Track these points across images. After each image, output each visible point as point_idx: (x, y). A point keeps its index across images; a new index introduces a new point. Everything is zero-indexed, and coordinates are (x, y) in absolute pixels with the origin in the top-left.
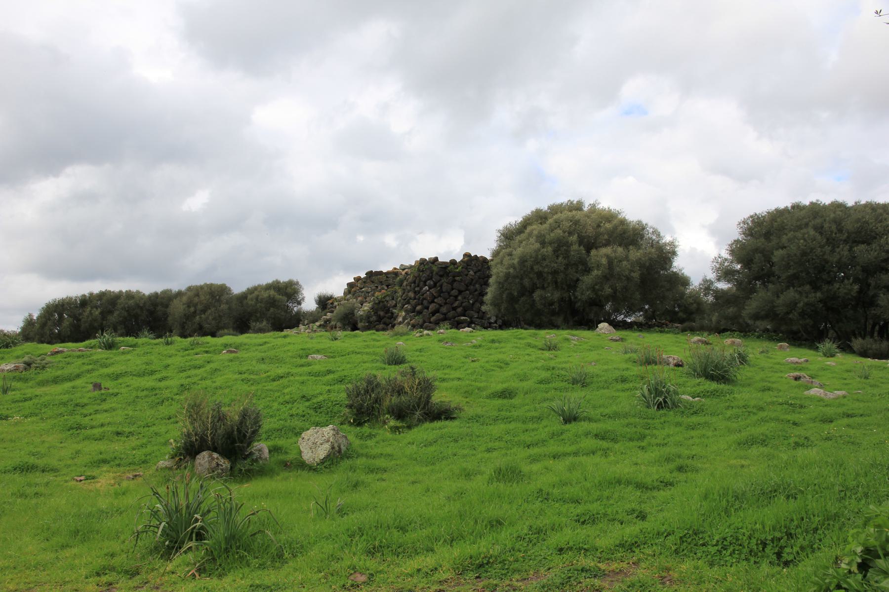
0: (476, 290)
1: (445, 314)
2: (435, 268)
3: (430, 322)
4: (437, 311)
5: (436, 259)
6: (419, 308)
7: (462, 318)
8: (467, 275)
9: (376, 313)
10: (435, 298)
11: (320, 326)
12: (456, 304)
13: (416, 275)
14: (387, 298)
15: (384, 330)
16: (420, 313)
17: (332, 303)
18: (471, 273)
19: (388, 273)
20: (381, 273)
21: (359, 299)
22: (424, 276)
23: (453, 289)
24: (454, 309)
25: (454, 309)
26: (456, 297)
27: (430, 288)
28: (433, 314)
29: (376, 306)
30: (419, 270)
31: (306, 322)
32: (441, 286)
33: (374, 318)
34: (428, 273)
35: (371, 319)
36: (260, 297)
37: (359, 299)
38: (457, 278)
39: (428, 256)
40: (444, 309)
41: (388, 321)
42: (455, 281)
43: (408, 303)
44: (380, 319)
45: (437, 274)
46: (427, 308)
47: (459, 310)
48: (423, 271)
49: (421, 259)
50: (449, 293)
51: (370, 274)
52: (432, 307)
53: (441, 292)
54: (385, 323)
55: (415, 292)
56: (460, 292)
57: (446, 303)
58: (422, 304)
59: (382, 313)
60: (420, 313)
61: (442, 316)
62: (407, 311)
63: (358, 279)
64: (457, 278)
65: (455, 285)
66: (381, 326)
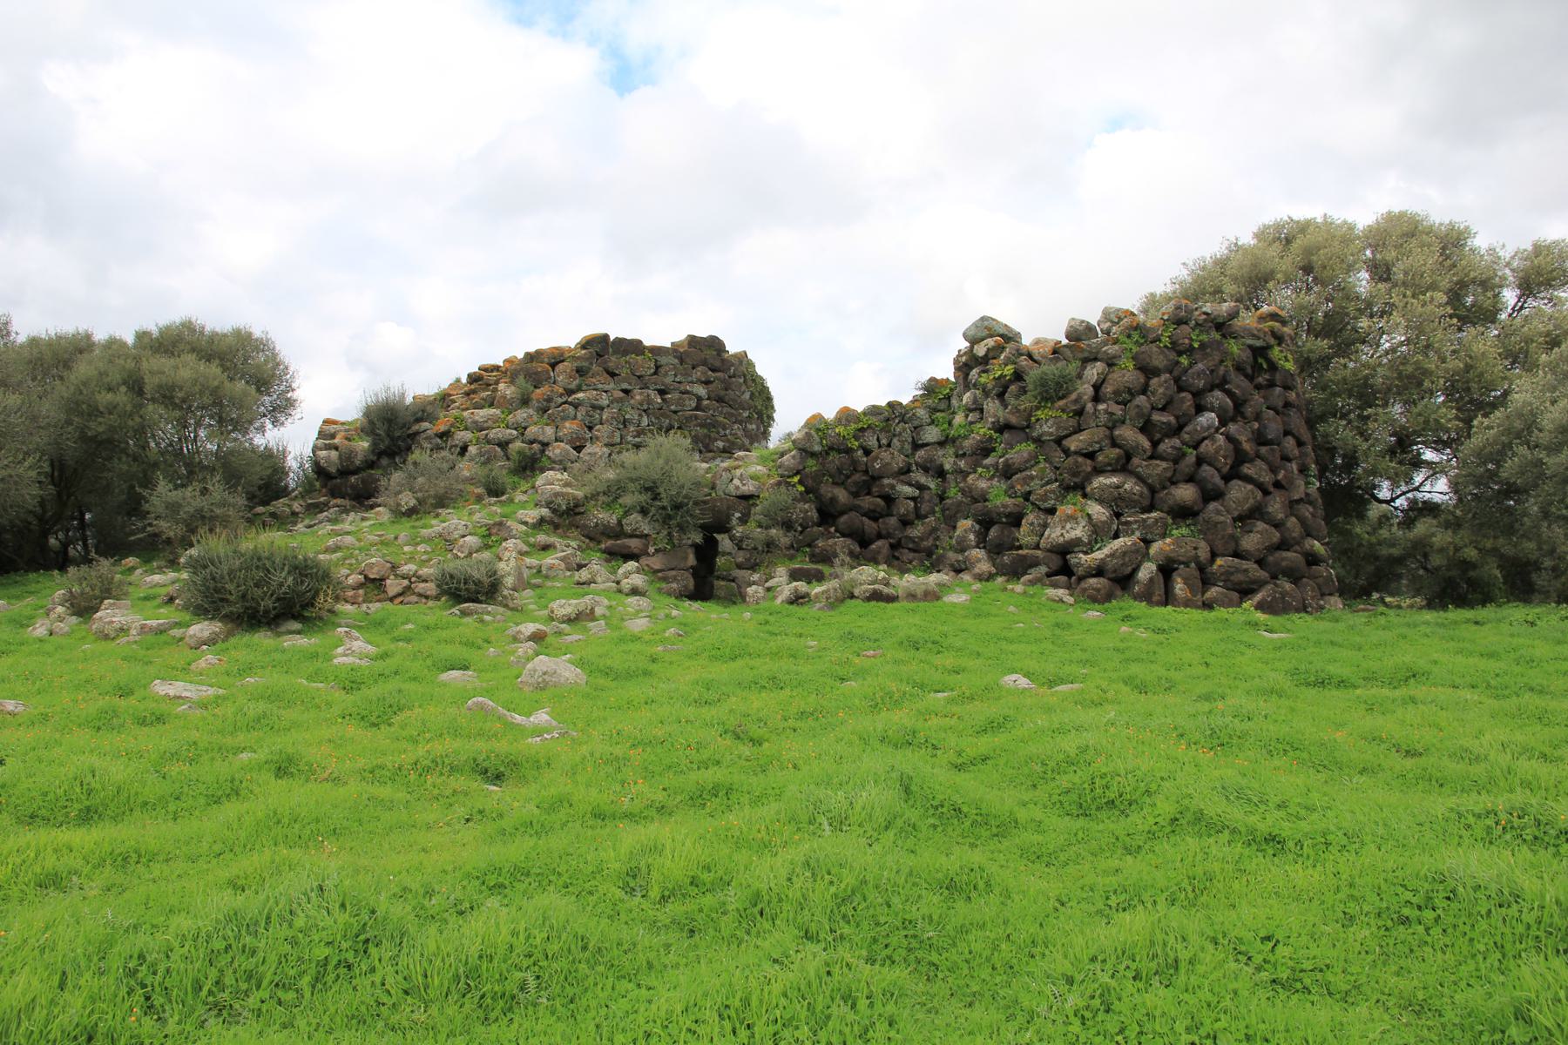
2: (1234, 348)
6: (1185, 493)
9: (811, 491)
14: (872, 442)
16: (1183, 513)
19: (657, 351)
20: (635, 347)
29: (812, 465)
31: (407, 500)
33: (809, 510)
36: (150, 383)
37: (569, 427)
41: (870, 526)
43: (1123, 466)
44: (827, 515)
51: (599, 346)
58: (1190, 479)
59: (842, 495)
62: (1118, 505)
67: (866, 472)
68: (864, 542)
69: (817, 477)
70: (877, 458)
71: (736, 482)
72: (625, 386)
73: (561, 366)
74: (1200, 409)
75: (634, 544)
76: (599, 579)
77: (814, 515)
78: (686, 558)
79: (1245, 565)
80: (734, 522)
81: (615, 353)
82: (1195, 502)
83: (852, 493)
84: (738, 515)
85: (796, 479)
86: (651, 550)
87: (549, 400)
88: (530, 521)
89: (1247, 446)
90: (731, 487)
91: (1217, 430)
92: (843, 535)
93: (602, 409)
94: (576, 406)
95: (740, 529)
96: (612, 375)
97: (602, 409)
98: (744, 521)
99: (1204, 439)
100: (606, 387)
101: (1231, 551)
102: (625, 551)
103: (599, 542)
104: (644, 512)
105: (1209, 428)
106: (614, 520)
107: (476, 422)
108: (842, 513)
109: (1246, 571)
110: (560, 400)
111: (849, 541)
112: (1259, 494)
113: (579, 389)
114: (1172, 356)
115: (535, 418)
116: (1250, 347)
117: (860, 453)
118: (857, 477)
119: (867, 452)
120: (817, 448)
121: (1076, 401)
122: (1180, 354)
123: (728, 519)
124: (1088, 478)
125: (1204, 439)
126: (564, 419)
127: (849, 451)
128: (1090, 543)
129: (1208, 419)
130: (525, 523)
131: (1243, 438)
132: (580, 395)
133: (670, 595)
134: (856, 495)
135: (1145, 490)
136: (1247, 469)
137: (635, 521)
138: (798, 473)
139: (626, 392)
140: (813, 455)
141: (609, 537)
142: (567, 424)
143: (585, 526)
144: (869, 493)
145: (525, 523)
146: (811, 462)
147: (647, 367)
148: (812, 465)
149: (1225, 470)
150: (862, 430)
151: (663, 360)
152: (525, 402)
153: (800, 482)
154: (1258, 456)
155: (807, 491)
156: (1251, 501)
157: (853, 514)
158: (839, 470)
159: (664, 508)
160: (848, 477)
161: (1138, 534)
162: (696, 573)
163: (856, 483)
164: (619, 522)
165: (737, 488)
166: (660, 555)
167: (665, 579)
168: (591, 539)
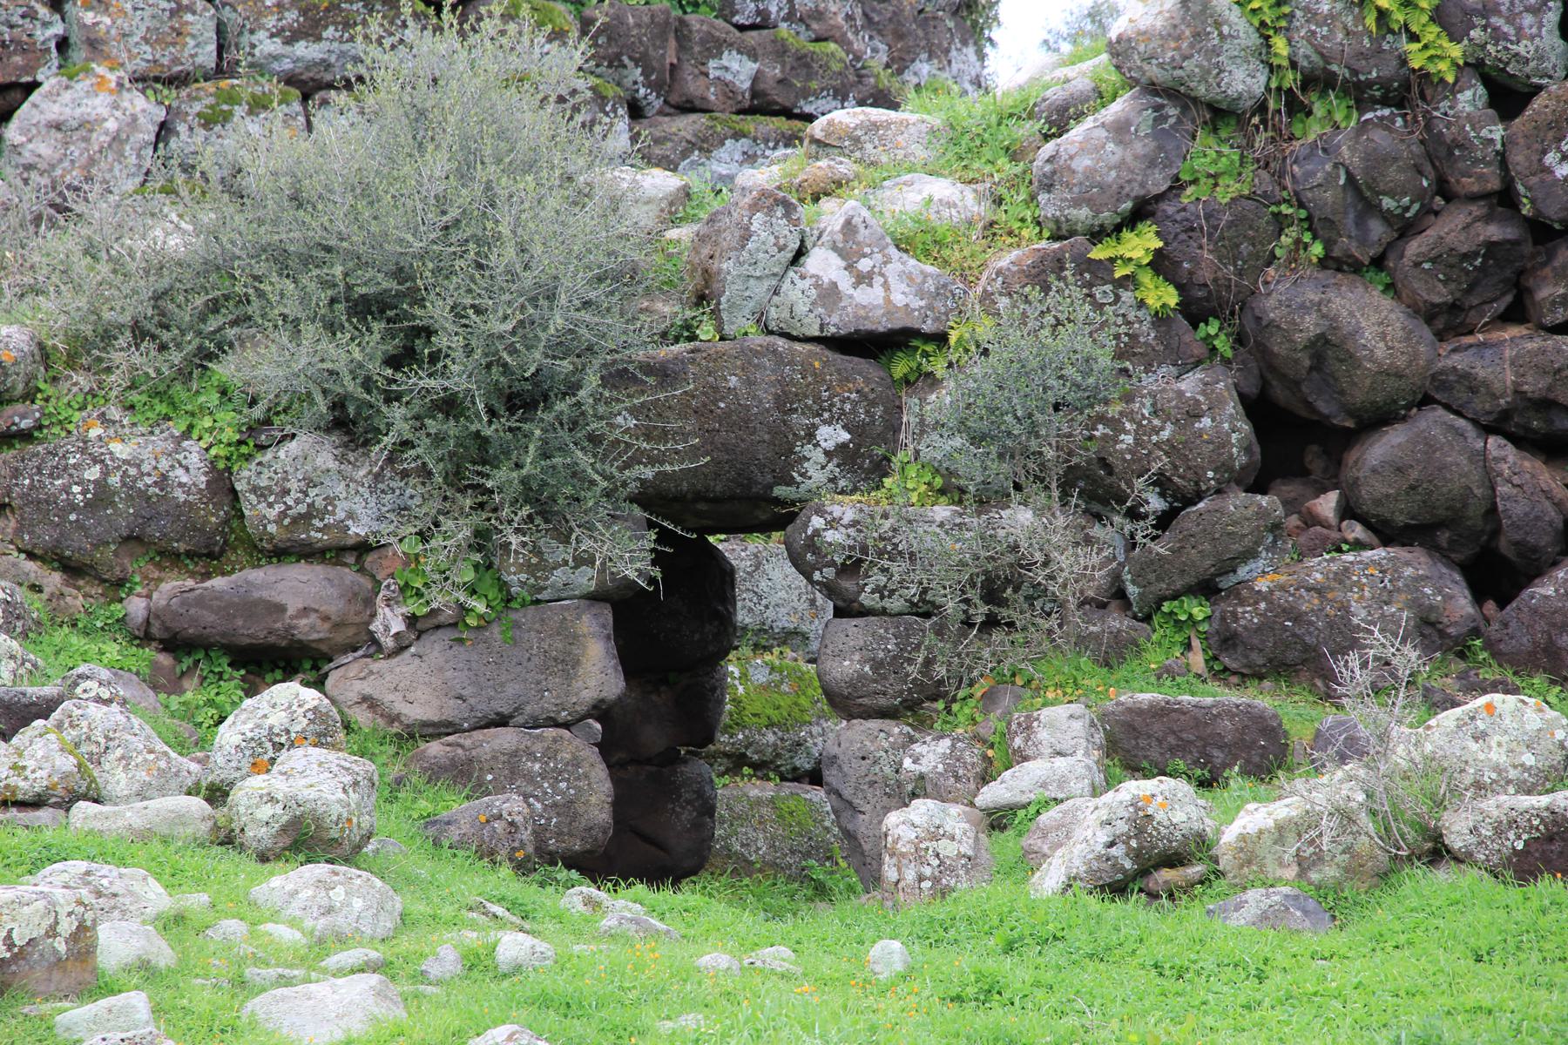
33: (1208, 409)
59: (1378, 326)
67: (1505, 199)
68: (1496, 572)
69: (1250, 231)
71: (823, 264)
75: (300, 593)
76: (117, 780)
77: (1229, 428)
78: (568, 664)
80: (815, 470)
83: (1429, 314)
84: (832, 435)
85: (1141, 244)
86: (390, 621)
90: (797, 294)
92: (1386, 533)
95: (845, 509)
98: (865, 463)
102: (251, 631)
103: (117, 586)
104: (348, 425)
106: (190, 472)
108: (1378, 419)
111: (1413, 564)
117: (1471, 98)
118: (1457, 229)
119: (1508, 96)
120: (1244, 82)
123: (785, 463)
127: (1408, 91)
133: (488, 854)
134: (1447, 321)
137: (304, 472)
138: (1141, 212)
140: (1219, 114)
141: (170, 558)
143: (42, 504)
144: (1516, 313)
146: (1210, 154)
148: (1217, 170)
153: (1161, 264)
155: (1193, 311)
157: (1434, 421)
158: (1362, 195)
159: (450, 406)
160: (1406, 228)
162: (616, 732)
163: (1446, 261)
164: (222, 485)
165: (829, 294)
166: (434, 648)
167: (461, 774)
168: (73, 569)
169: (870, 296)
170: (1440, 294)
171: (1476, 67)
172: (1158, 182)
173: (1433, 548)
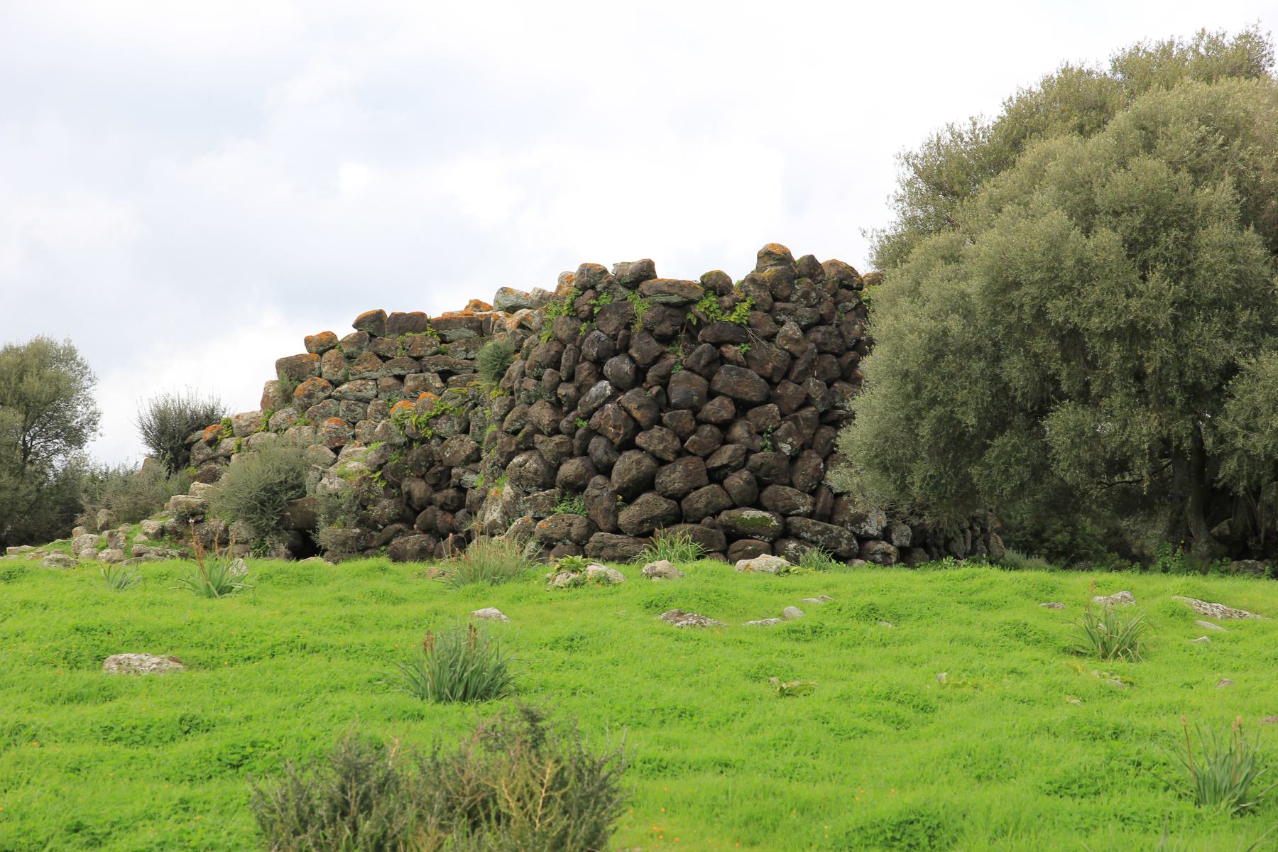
0: (807, 402)
1: (678, 497)
3: (617, 530)
4: (645, 484)
5: (646, 271)
6: (570, 469)
7: (749, 514)
8: (770, 338)
10: (638, 428)
11: (162, 532)
12: (725, 455)
13: (563, 333)
14: (443, 427)
15: (424, 555)
16: (575, 488)
17: (213, 442)
18: (791, 328)
19: (447, 322)
20: (415, 322)
21: (327, 425)
22: (594, 338)
23: (711, 395)
24: (716, 476)
25: (716, 476)
26: (725, 426)
27: (619, 389)
28: (630, 494)
30: (574, 314)
31: (102, 517)
32: (664, 381)
33: (385, 507)
34: (612, 324)
35: (375, 512)
37: (327, 425)
38: (730, 351)
39: (613, 255)
40: (673, 478)
41: (442, 519)
42: (723, 360)
44: (409, 513)
45: (648, 330)
46: (606, 470)
47: (737, 481)
48: (591, 317)
49: (586, 270)
50: (695, 410)
51: (373, 325)
52: (627, 466)
53: (662, 404)
54: (429, 530)
55: (557, 404)
56: (743, 407)
57: (681, 453)
58: (584, 452)
59: (418, 488)
60: (575, 488)
61: (664, 506)
63: (322, 345)
64: (730, 351)
65: (722, 378)
66: (415, 540)
69: (399, 472)
70: (447, 446)
71: (325, 481)
72: (397, 371)
73: (326, 355)
74: (601, 377)
79: (616, 538)
81: (392, 331)
82: (579, 477)
87: (310, 396)
88: (151, 531)
89: (637, 415)
91: (610, 399)
93: (367, 401)
94: (338, 399)
96: (384, 359)
97: (367, 401)
99: (596, 409)
100: (375, 375)
101: (609, 526)
105: (597, 398)
107: (239, 427)
108: (423, 508)
109: (614, 546)
110: (322, 395)
112: (647, 462)
113: (347, 380)
114: (573, 324)
115: (295, 418)
116: (666, 304)
120: (399, 440)
121: (509, 378)
122: (583, 320)
124: (510, 457)
125: (596, 409)
126: (325, 416)
127: (424, 441)
128: (504, 525)
129: (605, 387)
130: (146, 534)
131: (632, 406)
132: (344, 387)
134: (437, 487)
135: (541, 468)
136: (640, 439)
139: (401, 378)
142: (326, 423)
145: (146, 534)
147: (426, 343)
149: (617, 441)
150: (436, 417)
151: (451, 334)
152: (287, 398)
153: (382, 477)
154: (659, 422)
156: (634, 472)
160: (428, 469)
161: (531, 513)
165: (324, 487)
169: (332, 487)
170: (434, 481)
171: (433, 435)
172: (383, 461)
173: (431, 534)
